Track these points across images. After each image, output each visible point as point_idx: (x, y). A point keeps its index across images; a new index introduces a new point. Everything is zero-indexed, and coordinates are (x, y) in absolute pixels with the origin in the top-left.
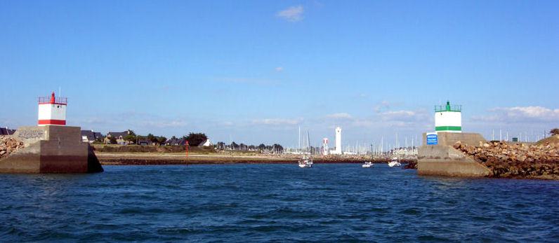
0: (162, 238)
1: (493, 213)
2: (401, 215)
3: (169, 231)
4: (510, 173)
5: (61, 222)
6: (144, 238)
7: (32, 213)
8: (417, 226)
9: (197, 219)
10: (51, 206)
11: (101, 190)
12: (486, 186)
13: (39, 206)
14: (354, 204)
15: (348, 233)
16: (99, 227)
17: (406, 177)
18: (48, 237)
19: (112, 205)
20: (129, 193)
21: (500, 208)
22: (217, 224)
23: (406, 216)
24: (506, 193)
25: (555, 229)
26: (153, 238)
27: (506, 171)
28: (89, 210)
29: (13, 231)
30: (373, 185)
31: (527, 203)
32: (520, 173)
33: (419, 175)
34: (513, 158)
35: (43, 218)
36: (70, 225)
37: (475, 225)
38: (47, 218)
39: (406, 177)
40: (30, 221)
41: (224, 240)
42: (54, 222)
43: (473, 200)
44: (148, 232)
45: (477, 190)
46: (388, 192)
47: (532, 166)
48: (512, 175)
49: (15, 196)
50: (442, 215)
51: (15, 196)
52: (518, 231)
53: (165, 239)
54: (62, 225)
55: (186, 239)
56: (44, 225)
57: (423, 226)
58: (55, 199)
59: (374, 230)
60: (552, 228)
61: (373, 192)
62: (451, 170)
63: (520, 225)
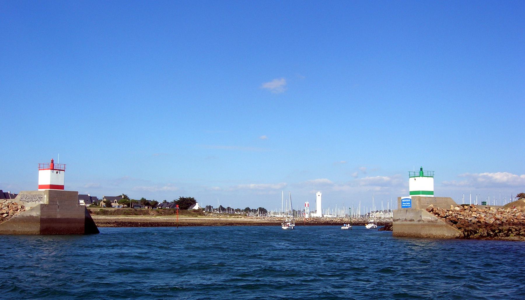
0: (154, 295)
1: (463, 272)
2: (377, 274)
3: (161, 289)
4: (479, 234)
5: (61, 280)
6: (136, 296)
7: (32, 272)
8: (393, 284)
9: (186, 278)
10: (50, 265)
11: (96, 251)
12: (457, 247)
13: (40, 265)
14: (334, 264)
15: (328, 291)
16: (95, 285)
17: (382, 238)
18: (48, 295)
19: (107, 264)
20: (123, 253)
21: (470, 267)
22: (205, 282)
23: (382, 274)
24: (475, 253)
25: (521, 286)
26: (146, 295)
27: (476, 233)
28: (85, 270)
29: (15, 289)
30: (351, 246)
31: (495, 263)
32: (489, 234)
33: (395, 236)
34: (482, 220)
35: (43, 277)
36: (68, 284)
37: (447, 283)
38: (46, 277)
39: (382, 238)
40: (31, 279)
41: (212, 297)
42: (54, 280)
43: (445, 260)
44: (141, 290)
45: (449, 250)
46: (365, 252)
47: (500, 228)
48: (482, 236)
49: (17, 256)
50: (417, 274)
51: (17, 256)
52: (487, 288)
53: (157, 296)
54: (61, 283)
55: (176, 297)
56: (44, 284)
57: (399, 283)
58: (54, 259)
59: (352, 287)
60: (518, 286)
61: (351, 252)
62: (424, 232)
63: (489, 283)
